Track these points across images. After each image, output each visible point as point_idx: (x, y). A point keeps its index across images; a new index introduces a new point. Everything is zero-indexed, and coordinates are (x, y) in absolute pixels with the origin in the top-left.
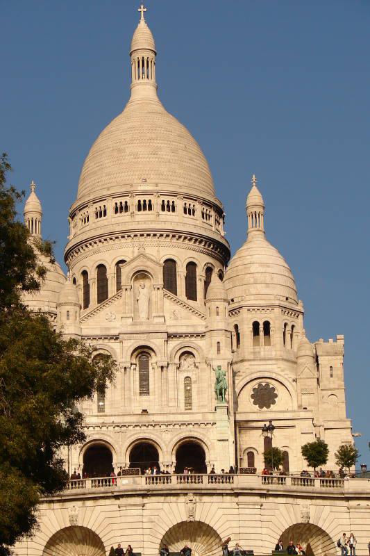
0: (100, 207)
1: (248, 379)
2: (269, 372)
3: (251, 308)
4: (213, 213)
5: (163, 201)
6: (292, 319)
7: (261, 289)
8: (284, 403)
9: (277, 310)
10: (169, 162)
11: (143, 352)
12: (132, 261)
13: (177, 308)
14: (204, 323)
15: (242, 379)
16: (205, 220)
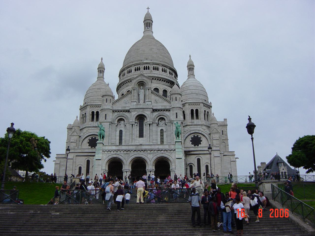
0: (129, 70)
1: (189, 133)
2: (198, 130)
3: (190, 104)
4: (173, 73)
5: (154, 67)
6: (207, 109)
7: (195, 96)
8: (204, 143)
9: (202, 105)
10: (157, 53)
11: (141, 118)
12: (137, 77)
13: (157, 98)
14: (170, 105)
15: (187, 133)
16: (170, 75)
